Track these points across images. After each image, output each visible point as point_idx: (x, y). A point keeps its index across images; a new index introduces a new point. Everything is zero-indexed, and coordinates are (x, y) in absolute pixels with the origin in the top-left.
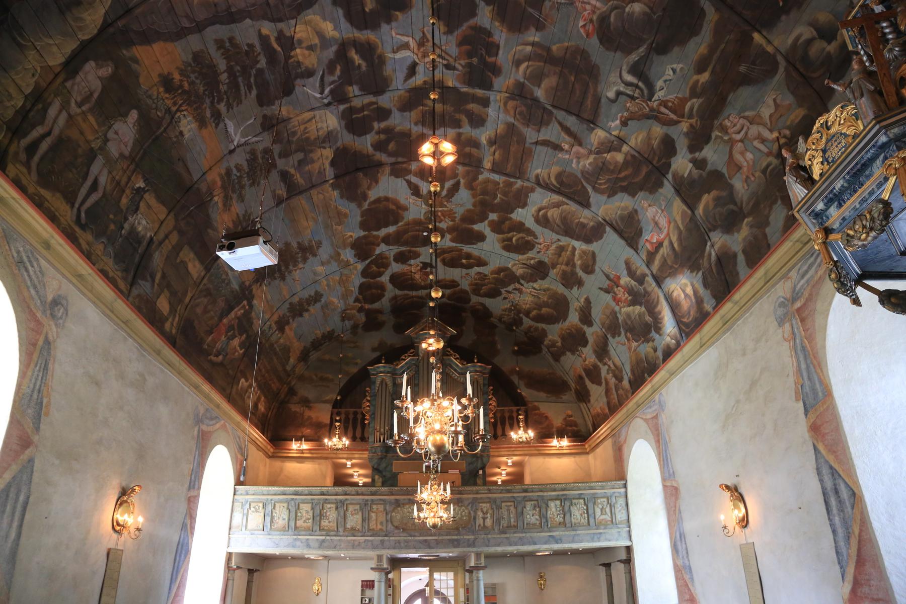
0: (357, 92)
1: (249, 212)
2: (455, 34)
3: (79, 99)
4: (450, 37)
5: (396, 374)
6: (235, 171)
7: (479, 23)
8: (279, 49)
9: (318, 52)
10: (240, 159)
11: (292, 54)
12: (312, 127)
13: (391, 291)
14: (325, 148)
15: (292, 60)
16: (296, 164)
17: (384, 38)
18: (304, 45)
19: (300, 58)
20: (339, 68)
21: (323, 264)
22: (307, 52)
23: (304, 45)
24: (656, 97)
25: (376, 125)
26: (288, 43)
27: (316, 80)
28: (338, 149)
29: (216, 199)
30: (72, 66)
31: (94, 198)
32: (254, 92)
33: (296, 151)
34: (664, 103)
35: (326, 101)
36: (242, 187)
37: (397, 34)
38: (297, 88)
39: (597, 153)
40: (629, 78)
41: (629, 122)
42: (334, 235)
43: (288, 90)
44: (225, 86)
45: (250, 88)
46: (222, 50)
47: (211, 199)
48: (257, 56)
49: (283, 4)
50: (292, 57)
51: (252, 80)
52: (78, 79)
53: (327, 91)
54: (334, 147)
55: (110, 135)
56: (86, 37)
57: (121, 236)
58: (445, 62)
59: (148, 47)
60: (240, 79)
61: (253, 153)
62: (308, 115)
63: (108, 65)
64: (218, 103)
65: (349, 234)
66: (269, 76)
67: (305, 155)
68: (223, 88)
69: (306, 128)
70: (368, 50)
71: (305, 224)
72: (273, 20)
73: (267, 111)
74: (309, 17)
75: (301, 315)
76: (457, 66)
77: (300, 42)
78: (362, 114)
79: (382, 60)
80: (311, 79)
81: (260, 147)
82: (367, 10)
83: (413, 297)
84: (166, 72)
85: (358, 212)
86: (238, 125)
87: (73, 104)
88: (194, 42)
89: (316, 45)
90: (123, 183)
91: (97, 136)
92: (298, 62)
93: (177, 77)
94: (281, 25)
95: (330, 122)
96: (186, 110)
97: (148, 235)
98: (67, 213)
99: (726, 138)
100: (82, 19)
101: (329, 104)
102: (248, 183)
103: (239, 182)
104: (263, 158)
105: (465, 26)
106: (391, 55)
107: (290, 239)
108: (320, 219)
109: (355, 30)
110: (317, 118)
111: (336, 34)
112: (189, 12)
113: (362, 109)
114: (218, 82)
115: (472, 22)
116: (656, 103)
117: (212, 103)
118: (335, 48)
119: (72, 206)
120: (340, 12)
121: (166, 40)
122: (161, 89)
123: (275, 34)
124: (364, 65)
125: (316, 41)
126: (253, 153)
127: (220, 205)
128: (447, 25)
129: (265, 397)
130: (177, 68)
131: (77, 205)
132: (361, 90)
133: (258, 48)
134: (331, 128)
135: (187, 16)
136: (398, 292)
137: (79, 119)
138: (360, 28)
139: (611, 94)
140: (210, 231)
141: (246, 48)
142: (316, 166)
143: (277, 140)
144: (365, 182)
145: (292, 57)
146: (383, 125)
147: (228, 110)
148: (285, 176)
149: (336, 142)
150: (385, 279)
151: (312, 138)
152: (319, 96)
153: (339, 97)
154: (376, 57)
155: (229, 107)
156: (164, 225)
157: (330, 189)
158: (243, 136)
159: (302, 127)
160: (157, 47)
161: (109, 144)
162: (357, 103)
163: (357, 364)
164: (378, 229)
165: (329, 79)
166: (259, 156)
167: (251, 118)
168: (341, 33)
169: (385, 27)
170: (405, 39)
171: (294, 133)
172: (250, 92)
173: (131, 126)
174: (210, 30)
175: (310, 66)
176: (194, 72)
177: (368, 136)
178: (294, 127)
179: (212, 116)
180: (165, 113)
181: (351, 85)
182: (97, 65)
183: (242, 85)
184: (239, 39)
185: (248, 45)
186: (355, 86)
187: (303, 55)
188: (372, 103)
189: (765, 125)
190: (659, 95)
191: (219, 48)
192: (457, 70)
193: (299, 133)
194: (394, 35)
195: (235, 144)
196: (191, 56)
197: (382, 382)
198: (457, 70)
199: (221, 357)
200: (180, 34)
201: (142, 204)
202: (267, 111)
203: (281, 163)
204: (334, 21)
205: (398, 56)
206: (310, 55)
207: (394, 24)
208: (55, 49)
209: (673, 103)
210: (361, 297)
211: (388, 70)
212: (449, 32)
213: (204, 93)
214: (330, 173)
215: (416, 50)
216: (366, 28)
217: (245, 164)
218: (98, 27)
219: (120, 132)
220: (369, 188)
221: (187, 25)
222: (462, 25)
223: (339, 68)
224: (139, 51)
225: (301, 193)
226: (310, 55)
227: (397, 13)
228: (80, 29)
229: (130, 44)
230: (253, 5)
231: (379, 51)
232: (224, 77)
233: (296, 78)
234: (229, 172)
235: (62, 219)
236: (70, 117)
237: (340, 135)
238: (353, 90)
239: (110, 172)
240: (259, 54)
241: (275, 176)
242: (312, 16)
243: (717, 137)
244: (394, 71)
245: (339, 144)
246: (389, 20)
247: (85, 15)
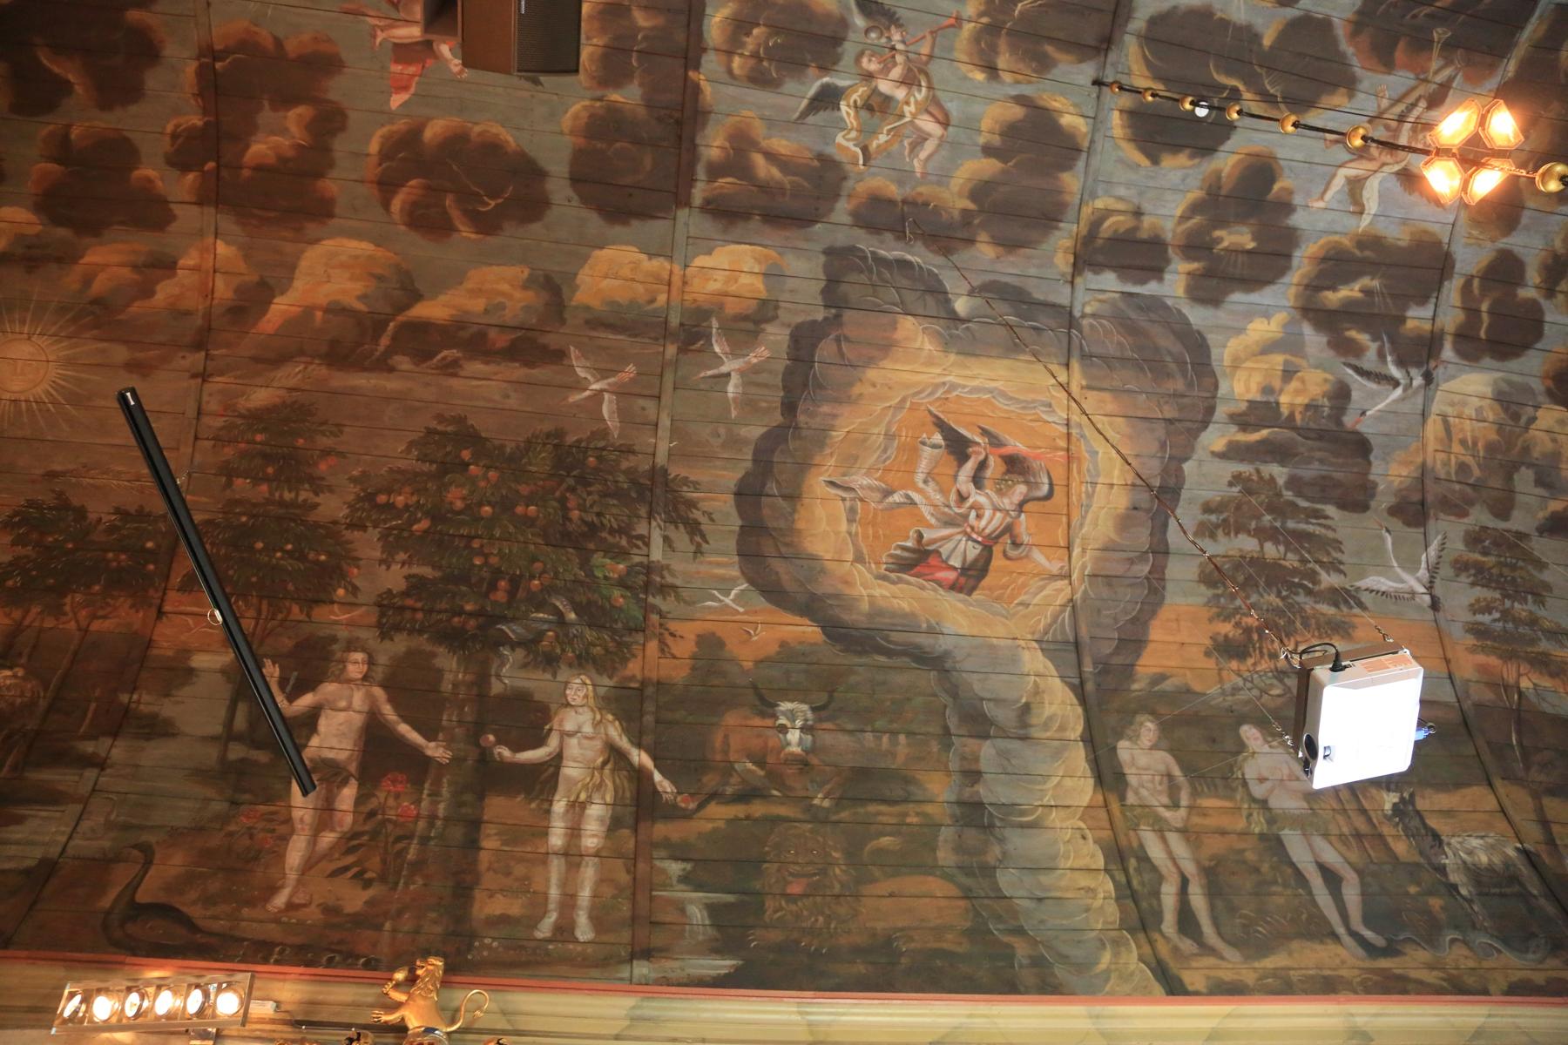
0: (1427, 312)
2: (1358, 71)
3: (1165, 800)
4: (1365, 85)
6: (1485, 618)
7: (1349, 15)
8: (1265, 432)
9: (1304, 363)
10: (1461, 597)
11: (1285, 411)
12: (1468, 428)
14: (1533, 419)
15: (1298, 417)
16: (1540, 491)
17: (1321, 226)
18: (1277, 384)
19: (1301, 400)
20: (1353, 334)
22: (1294, 384)
23: (1277, 384)
25: (1527, 293)
26: (1260, 413)
27: (1360, 387)
28: (1549, 393)
29: (1525, 684)
30: (1108, 776)
31: (1352, 894)
32: (1331, 510)
33: (1509, 478)
35: (1418, 381)
36: (1533, 622)
37: (1322, 198)
38: (1361, 428)
43: (1361, 447)
44: (1290, 555)
45: (1318, 514)
46: (1220, 532)
47: (1520, 694)
48: (1261, 478)
49: (1183, 396)
50: (1292, 416)
51: (1303, 504)
52: (1133, 780)
53: (1395, 371)
54: (1541, 398)
55: (1258, 791)
56: (1080, 728)
57: (1470, 901)
58: (1423, 104)
59: (1151, 647)
60: (1291, 524)
61: (1461, 566)
62: (1433, 428)
63: (1142, 724)
64: (1316, 582)
66: (1309, 472)
67: (1530, 465)
68: (1292, 561)
69: (1463, 442)
70: (1337, 266)
72: (1205, 424)
73: (1383, 501)
74: (1227, 361)
76: (1439, 78)
77: (1267, 390)
78: (1485, 317)
79: (1371, 242)
80: (1355, 395)
81: (1458, 546)
82: (1251, 245)
84: (1208, 642)
86: (1384, 568)
87: (1167, 814)
88: (1181, 571)
89: (1286, 362)
90: (1363, 827)
91: (1245, 813)
92: (1307, 407)
93: (1226, 628)
94: (1221, 411)
95: (1471, 389)
96: (1297, 644)
97: (1511, 853)
98: (1342, 957)
100: (1051, 718)
101: (1428, 378)
102: (1530, 606)
103: (1517, 621)
104: (1485, 553)
105: (1346, 47)
106: (1365, 221)
109: (1286, 280)
110: (1449, 410)
111: (1280, 318)
112: (1125, 555)
113: (1472, 312)
114: (1276, 565)
115: (1341, 31)
117: (1309, 592)
118: (1307, 330)
119: (1335, 937)
120: (1237, 297)
121: (1153, 613)
122: (1234, 664)
123: (1234, 428)
124: (1366, 281)
125: (1278, 360)
126: (1461, 566)
127: (1546, 682)
128: (1332, 86)
130: (1211, 620)
131: (1341, 930)
132: (1422, 300)
133: (1245, 468)
134: (1488, 391)
135: (1131, 561)
137: (1196, 820)
138: (1284, 270)
141: (1236, 490)
143: (1457, 508)
145: (1292, 416)
146: (1533, 276)
147: (1341, 572)
149: (1528, 390)
151: (1494, 437)
152: (1399, 391)
153: (1420, 353)
154: (1358, 253)
155: (1335, 567)
156: (1511, 812)
158: (1412, 567)
159: (1457, 448)
160: (1156, 632)
161: (1273, 803)
162: (1450, 315)
165: (1370, 360)
166: (1477, 557)
167: (1383, 540)
168: (1279, 308)
169: (1298, 219)
170: (1339, 182)
171: (1463, 468)
172: (1327, 517)
173: (1266, 748)
174: (1173, 536)
175: (1327, 387)
176: (1233, 597)
177: (1548, 317)
178: (1446, 464)
179: (1336, 605)
180: (1281, 681)
181: (1403, 320)
182: (1130, 739)
183: (1302, 526)
184: (1213, 494)
185: (1231, 484)
186: (1410, 313)
187: (1298, 392)
188: (1466, 289)
191: (1213, 536)
192: (1451, 79)
193: (1469, 460)
194: (1321, 204)
195: (1423, 590)
196: (1203, 588)
198: (1451, 79)
200: (1155, 587)
201: (1433, 822)
202: (1383, 501)
203: (1519, 521)
204: (1250, 315)
205: (1372, 205)
206: (1303, 381)
207: (1297, 200)
208: (1068, 782)
211: (1397, 234)
212: (1349, 84)
213: (1283, 599)
215: (1372, 166)
216: (1289, 257)
217: (1480, 592)
218: (1075, 701)
219: (1266, 774)
221: (1147, 568)
222: (1343, 55)
223: (1353, 334)
224: (1149, 664)
226: (1303, 381)
227: (1276, 187)
228: (1062, 728)
229: (1128, 671)
230: (1163, 446)
231: (1346, 242)
232: (1271, 551)
233: (1339, 423)
234: (1479, 631)
235: (1344, 973)
236: (1183, 831)
237: (1516, 378)
238: (1418, 318)
239: (1326, 836)
240: (1258, 471)
241: (1542, 547)
242: (1225, 351)
244: (1405, 221)
245: (1537, 385)
246: (1287, 207)
247: (1048, 711)
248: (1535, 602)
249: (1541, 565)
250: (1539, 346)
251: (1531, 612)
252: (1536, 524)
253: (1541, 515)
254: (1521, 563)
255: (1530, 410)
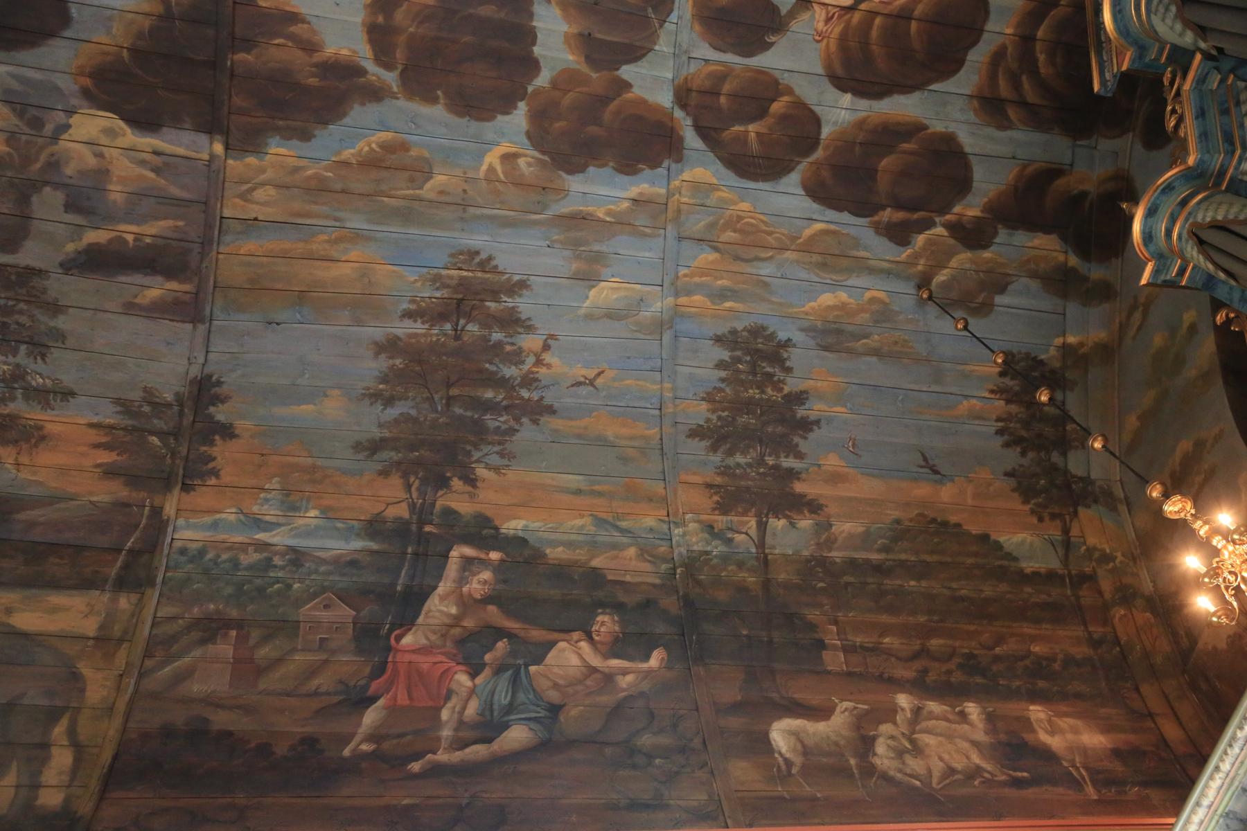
1: (136, 395)
5: (1222, 173)
13: (942, 108)
21: (588, 278)
28: (86, 94)
36: (18, 375)
42: (464, 206)
54: (74, 101)
65: (492, 158)
67: (57, 186)
71: (345, 270)
75: (806, 426)
83: (1026, 40)
85: (402, 103)
107: (376, 332)
108: (356, 222)
129: (1035, 696)
136: (966, 80)
140: (21, 516)
142: (123, 167)
144: (277, 53)
148: (98, 261)
150: (840, 112)
157: (251, 160)
163: (1193, 329)
164: (533, 66)
197: (1201, 242)
199: (517, 735)
210: (887, 215)
214: (181, 143)
220: (310, 47)
225: (206, 243)
245: (66, 83)
248: (29, 354)
249: (56, 308)
250: (67, 33)
251: (18, 366)
252: (61, 258)
253: (70, 247)
254: (22, 306)
255: (60, 117)
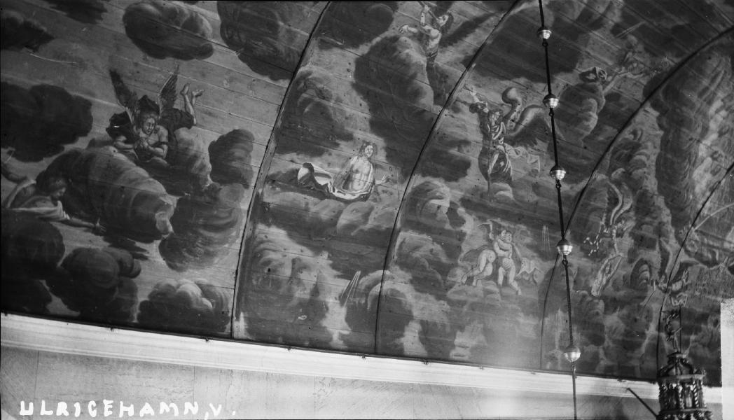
24: (508, 147)
34: (502, 157)
39: (429, 68)
40: (530, 116)
41: (476, 115)
99: (491, 236)
116: (502, 148)
139: (513, 94)
189: (518, 271)
190: (510, 151)
209: (504, 166)
243: (488, 226)
